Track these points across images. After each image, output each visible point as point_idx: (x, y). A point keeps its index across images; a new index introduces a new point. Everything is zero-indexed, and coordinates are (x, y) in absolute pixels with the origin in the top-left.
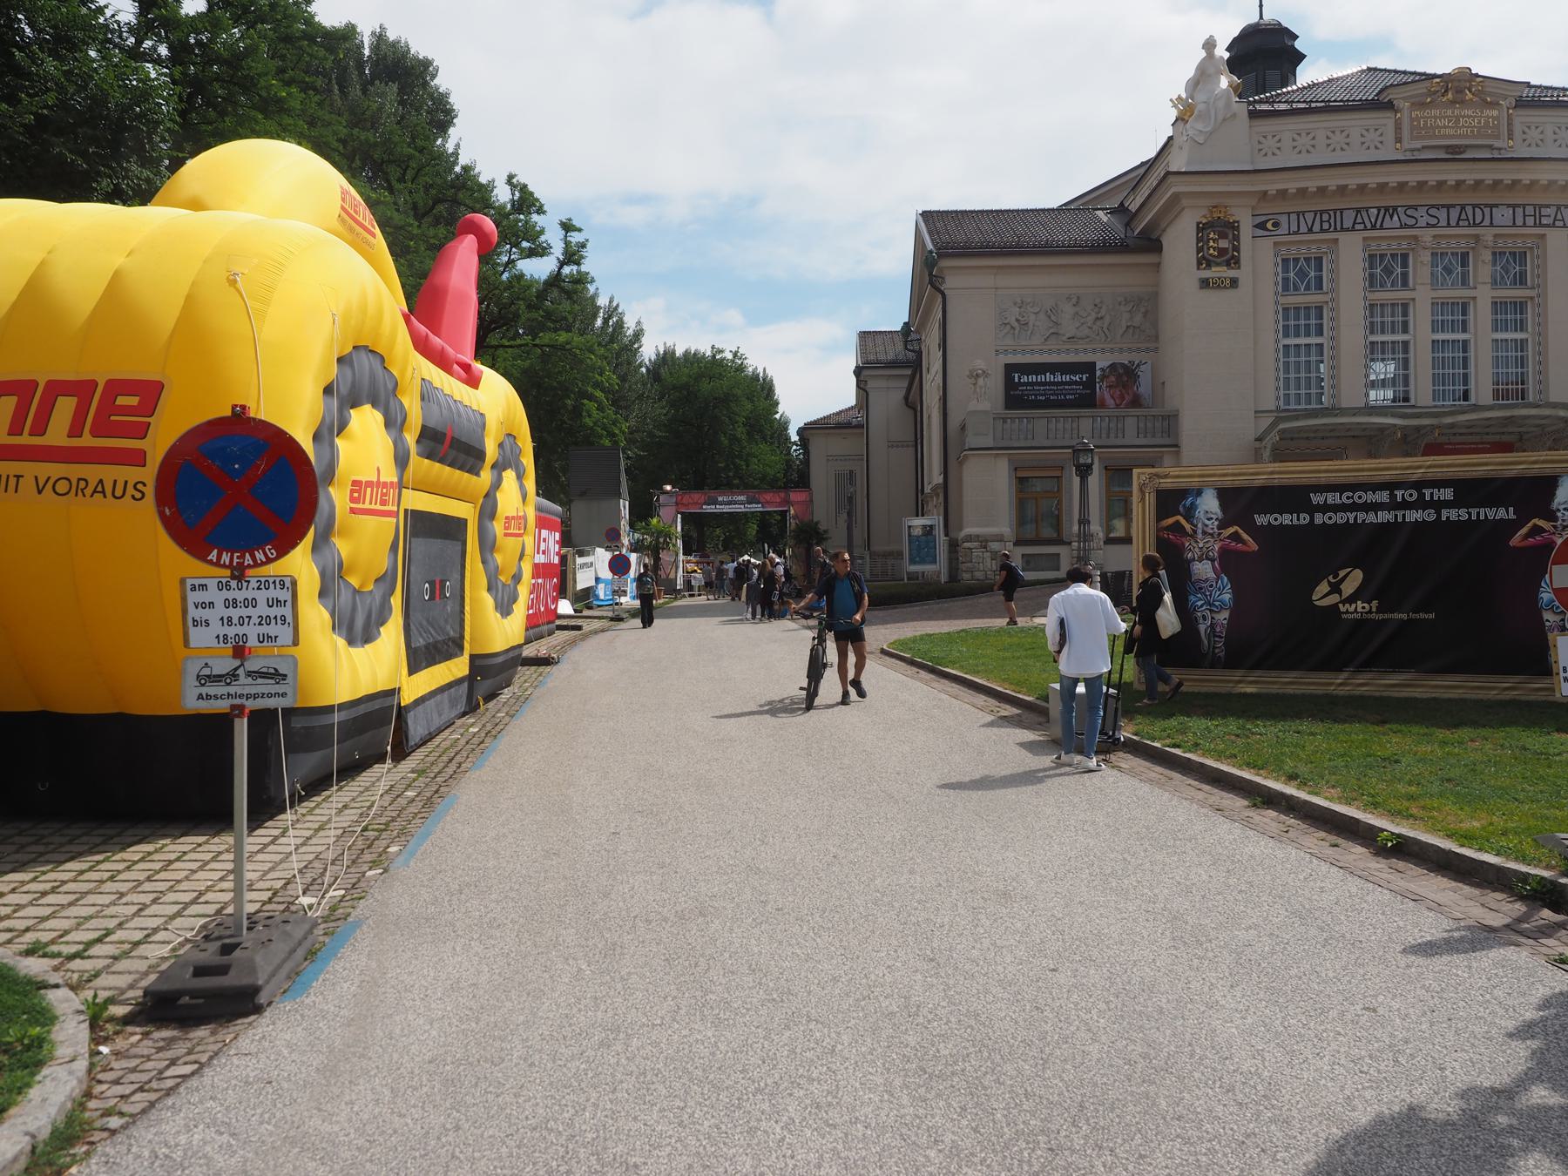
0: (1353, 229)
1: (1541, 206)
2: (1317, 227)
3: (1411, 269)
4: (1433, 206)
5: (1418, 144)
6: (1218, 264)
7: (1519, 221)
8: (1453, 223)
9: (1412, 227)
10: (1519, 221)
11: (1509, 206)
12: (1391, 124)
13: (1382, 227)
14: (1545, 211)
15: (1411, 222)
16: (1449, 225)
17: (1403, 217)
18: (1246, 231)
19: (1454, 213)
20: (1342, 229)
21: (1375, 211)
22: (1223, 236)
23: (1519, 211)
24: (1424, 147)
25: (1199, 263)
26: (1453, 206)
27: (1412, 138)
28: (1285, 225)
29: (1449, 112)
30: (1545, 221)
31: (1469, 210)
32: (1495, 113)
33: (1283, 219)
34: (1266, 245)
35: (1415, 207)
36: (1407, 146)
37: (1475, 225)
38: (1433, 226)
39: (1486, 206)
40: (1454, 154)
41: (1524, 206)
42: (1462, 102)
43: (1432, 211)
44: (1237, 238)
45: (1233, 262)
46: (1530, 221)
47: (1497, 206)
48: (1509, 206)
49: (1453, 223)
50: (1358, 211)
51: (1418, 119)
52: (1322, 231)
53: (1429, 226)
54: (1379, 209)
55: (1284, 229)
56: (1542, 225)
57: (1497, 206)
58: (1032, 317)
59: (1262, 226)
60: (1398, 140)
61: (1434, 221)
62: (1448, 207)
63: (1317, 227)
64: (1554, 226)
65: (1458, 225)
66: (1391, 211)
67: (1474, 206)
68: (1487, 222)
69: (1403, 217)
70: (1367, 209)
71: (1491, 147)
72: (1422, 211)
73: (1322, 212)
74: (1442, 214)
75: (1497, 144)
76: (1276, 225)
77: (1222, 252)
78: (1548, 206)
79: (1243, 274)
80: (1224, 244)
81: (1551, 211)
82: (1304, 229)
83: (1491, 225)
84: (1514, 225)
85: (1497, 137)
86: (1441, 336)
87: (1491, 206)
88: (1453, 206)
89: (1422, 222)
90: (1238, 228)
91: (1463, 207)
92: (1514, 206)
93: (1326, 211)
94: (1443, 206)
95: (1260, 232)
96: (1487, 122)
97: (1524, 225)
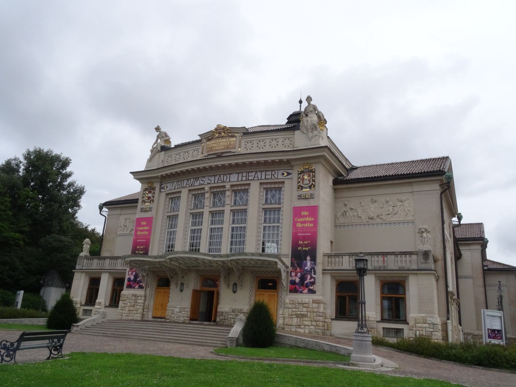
2: (176, 188)
5: (206, 154)
6: (148, 202)
7: (240, 179)
8: (216, 182)
9: (202, 184)
10: (240, 179)
12: (201, 148)
14: (250, 174)
15: (202, 182)
20: (184, 187)
22: (150, 192)
23: (240, 175)
24: (209, 155)
26: (216, 175)
28: (169, 187)
29: (217, 141)
30: (250, 178)
32: (234, 139)
35: (204, 177)
36: (204, 155)
37: (224, 182)
40: (219, 156)
42: (222, 137)
43: (210, 178)
44: (154, 193)
46: (244, 178)
47: (232, 174)
48: (236, 173)
49: (216, 182)
51: (208, 145)
52: (178, 188)
53: (208, 183)
56: (249, 180)
58: (128, 223)
61: (209, 182)
63: (176, 188)
68: (228, 181)
71: (230, 152)
72: (207, 178)
74: (212, 179)
75: (232, 151)
76: (167, 187)
77: (149, 198)
78: (252, 172)
79: (154, 205)
80: (150, 195)
81: (253, 174)
82: (173, 188)
85: (235, 148)
89: (206, 183)
90: (154, 189)
96: (230, 143)
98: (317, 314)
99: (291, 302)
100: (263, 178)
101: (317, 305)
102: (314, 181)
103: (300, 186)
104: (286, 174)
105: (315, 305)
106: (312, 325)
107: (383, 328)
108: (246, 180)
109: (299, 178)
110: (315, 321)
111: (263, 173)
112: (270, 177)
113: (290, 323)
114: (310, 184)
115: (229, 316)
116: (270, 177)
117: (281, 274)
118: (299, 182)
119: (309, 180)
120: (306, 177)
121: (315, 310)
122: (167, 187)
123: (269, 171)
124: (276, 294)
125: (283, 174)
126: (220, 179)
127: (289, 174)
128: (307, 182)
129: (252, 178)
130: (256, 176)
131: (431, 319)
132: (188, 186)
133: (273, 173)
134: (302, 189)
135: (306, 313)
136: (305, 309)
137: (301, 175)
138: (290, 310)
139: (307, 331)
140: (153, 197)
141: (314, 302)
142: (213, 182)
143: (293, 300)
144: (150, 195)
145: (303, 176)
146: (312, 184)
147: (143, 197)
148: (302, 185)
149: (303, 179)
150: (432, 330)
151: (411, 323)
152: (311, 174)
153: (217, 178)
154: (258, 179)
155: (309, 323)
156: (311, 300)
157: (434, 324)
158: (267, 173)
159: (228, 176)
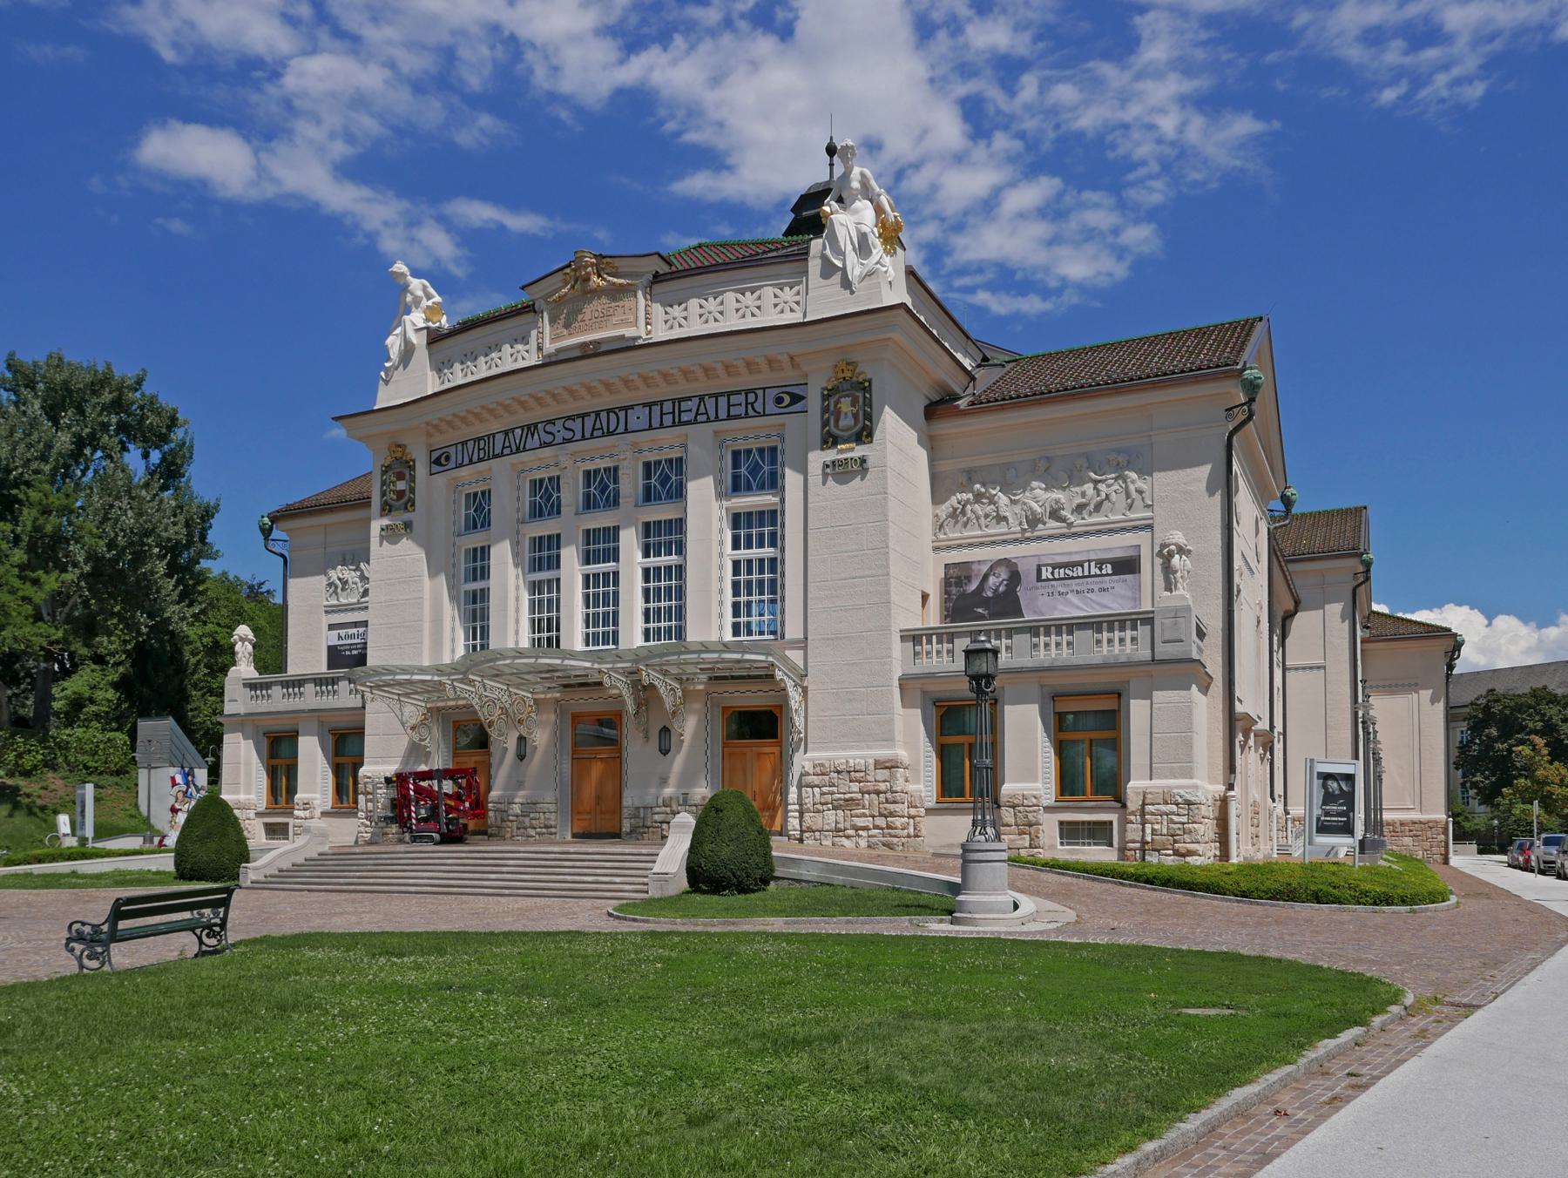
0: (502, 455)
1: (680, 400)
2: (475, 458)
3: (641, 482)
4: (569, 418)
7: (656, 423)
8: (587, 435)
10: (656, 423)
11: (644, 405)
13: (525, 450)
14: (684, 406)
15: (549, 438)
16: (583, 438)
17: (542, 433)
18: (421, 470)
19: (589, 422)
20: (495, 456)
21: (519, 431)
22: (401, 477)
23: (656, 409)
25: (383, 510)
27: (553, 340)
30: (685, 418)
31: (604, 415)
33: (452, 450)
34: (441, 480)
37: (610, 433)
38: (570, 441)
39: (621, 409)
40: (590, 352)
41: (662, 403)
43: (569, 424)
45: (409, 505)
46: (668, 420)
48: (644, 405)
49: (587, 435)
50: (506, 433)
53: (566, 441)
54: (522, 428)
55: (452, 464)
56: (681, 424)
57: (632, 407)
59: (437, 462)
60: (540, 349)
61: (569, 435)
62: (583, 416)
63: (475, 458)
64: (695, 422)
65: (592, 437)
66: (531, 428)
67: (609, 411)
68: (621, 428)
69: (542, 433)
70: (513, 430)
73: (480, 439)
77: (400, 494)
78: (689, 399)
80: (401, 485)
83: (626, 431)
84: (651, 428)
86: (653, 561)
87: (626, 409)
88: (588, 414)
89: (559, 439)
90: (412, 468)
91: (598, 414)
92: (650, 405)
93: (482, 438)
94: (578, 416)
95: (436, 468)
97: (662, 426)
98: (889, 795)
99: (818, 770)
100: (723, 414)
101: (886, 772)
102: (868, 416)
103: (830, 434)
104: (787, 399)
105: (882, 774)
106: (876, 827)
107: (1061, 823)
108: (674, 425)
109: (825, 410)
110: (881, 815)
111: (723, 401)
112: (741, 410)
113: (819, 826)
114: (860, 425)
115: (656, 817)
116: (741, 410)
117: (786, 698)
118: (825, 423)
119: (855, 416)
120: (845, 405)
121: (882, 787)
122: (448, 458)
123: (738, 393)
124: (776, 750)
125: (779, 400)
126: (598, 425)
127: (796, 399)
128: (849, 421)
129: (691, 416)
130: (702, 410)
131: (1182, 792)
132: (507, 451)
133: (751, 398)
134: (835, 444)
135: (859, 796)
136: (855, 787)
137: (832, 401)
138: (817, 790)
139: (863, 843)
140: (412, 490)
141: (879, 765)
142: (578, 436)
143: (822, 765)
144: (401, 485)
145: (837, 403)
146: (864, 428)
147: (383, 494)
148: (836, 432)
149: (837, 414)
150: (1184, 819)
151: (1133, 803)
152: (860, 395)
153: (589, 422)
154: (708, 420)
155: (868, 822)
156: (871, 761)
157: (1189, 803)
158: (734, 399)
159: (622, 414)
